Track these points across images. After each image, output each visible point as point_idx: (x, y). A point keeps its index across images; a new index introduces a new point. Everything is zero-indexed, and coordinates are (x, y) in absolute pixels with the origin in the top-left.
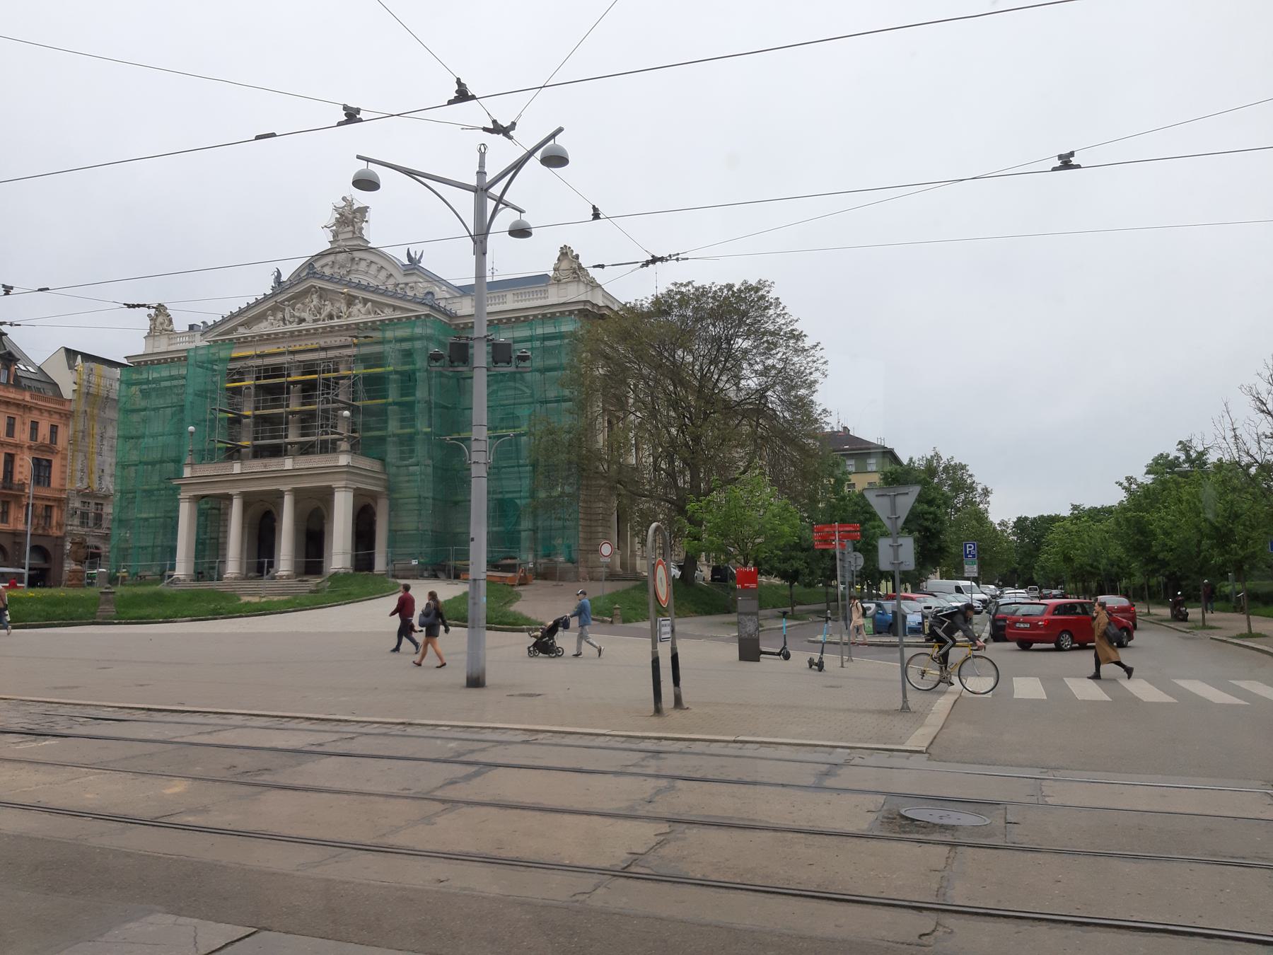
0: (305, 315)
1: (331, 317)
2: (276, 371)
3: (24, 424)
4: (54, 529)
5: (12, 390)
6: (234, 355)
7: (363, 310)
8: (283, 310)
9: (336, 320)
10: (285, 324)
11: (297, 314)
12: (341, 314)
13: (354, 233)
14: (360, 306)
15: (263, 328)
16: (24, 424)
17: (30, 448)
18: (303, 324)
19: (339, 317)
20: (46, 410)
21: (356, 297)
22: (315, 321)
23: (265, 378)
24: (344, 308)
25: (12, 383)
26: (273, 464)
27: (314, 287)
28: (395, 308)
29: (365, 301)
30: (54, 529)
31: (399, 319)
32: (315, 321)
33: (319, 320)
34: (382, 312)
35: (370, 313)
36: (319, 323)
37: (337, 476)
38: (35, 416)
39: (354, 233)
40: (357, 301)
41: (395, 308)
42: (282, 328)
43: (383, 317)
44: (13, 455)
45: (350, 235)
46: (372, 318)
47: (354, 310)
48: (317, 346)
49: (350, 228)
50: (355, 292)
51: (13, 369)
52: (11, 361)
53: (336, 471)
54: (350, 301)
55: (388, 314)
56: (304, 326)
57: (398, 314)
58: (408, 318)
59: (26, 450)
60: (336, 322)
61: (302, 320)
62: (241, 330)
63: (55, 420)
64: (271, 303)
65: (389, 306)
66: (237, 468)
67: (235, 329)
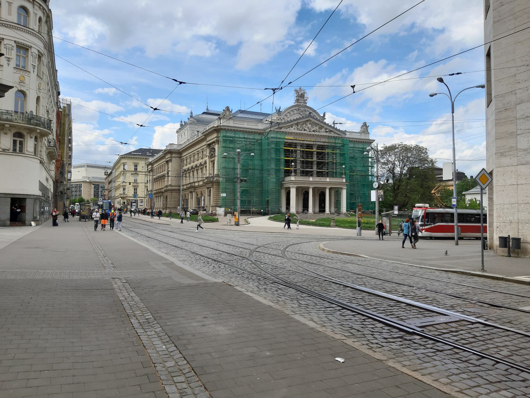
1: (314, 131)
2: (309, 146)
6: (286, 138)
14: (324, 130)
15: (292, 130)
19: (316, 132)
23: (306, 148)
26: (322, 179)
37: (343, 185)
41: (335, 133)
43: (330, 135)
48: (314, 140)
50: (324, 125)
53: (341, 183)
54: (321, 127)
55: (332, 134)
57: (336, 135)
60: (316, 133)
61: (305, 130)
64: (296, 122)
66: (311, 179)
67: (281, 128)
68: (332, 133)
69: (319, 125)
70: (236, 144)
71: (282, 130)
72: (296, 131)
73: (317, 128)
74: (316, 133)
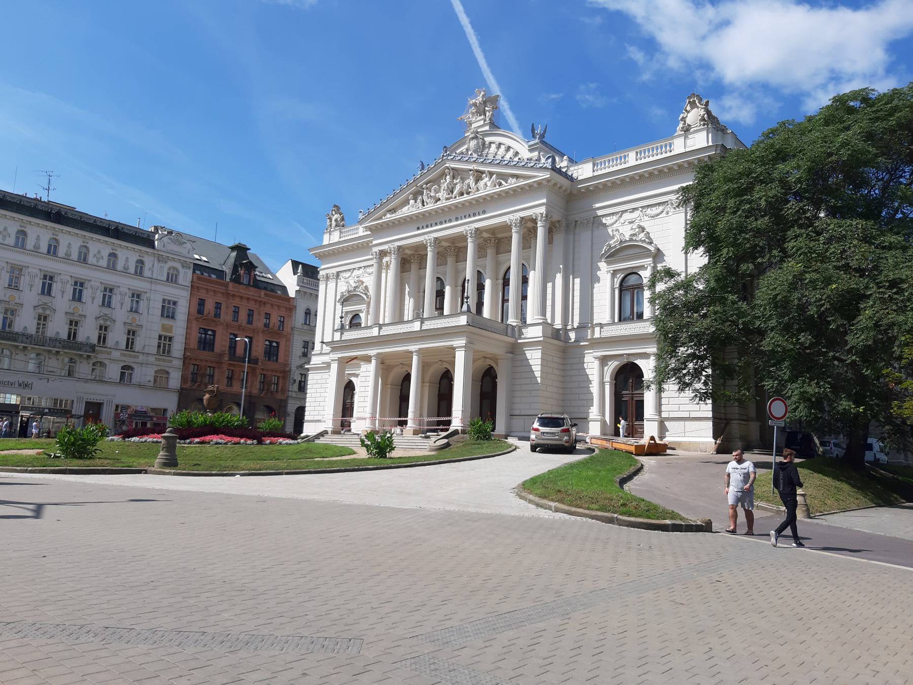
0: (440, 195)
1: (462, 194)
3: (259, 314)
4: (280, 393)
5: (251, 289)
7: (489, 184)
8: (422, 194)
9: (465, 195)
10: (424, 205)
11: (432, 194)
12: (470, 190)
13: (485, 120)
15: (406, 211)
16: (259, 314)
17: (263, 332)
18: (438, 203)
19: (468, 193)
20: (276, 305)
21: (482, 172)
22: (447, 199)
24: (472, 185)
25: (252, 284)
27: (448, 168)
28: (517, 177)
29: (491, 174)
30: (280, 393)
31: (522, 188)
32: (447, 199)
33: (452, 198)
34: (506, 183)
35: (495, 186)
36: (451, 200)
38: (267, 309)
39: (485, 120)
40: (484, 175)
41: (517, 177)
42: (422, 210)
43: (506, 186)
44: (252, 337)
45: (482, 123)
46: (498, 189)
47: (481, 184)
49: (482, 117)
51: (252, 274)
52: (252, 268)
54: (479, 176)
55: (512, 183)
56: (439, 205)
57: (522, 182)
58: (530, 186)
59: (261, 335)
60: (466, 197)
62: (388, 216)
63: (283, 312)
65: (513, 176)
68: (510, 180)
69: (471, 170)
70: (342, 279)
71: (384, 220)
72: (414, 211)
73: (471, 181)
74: (466, 197)
